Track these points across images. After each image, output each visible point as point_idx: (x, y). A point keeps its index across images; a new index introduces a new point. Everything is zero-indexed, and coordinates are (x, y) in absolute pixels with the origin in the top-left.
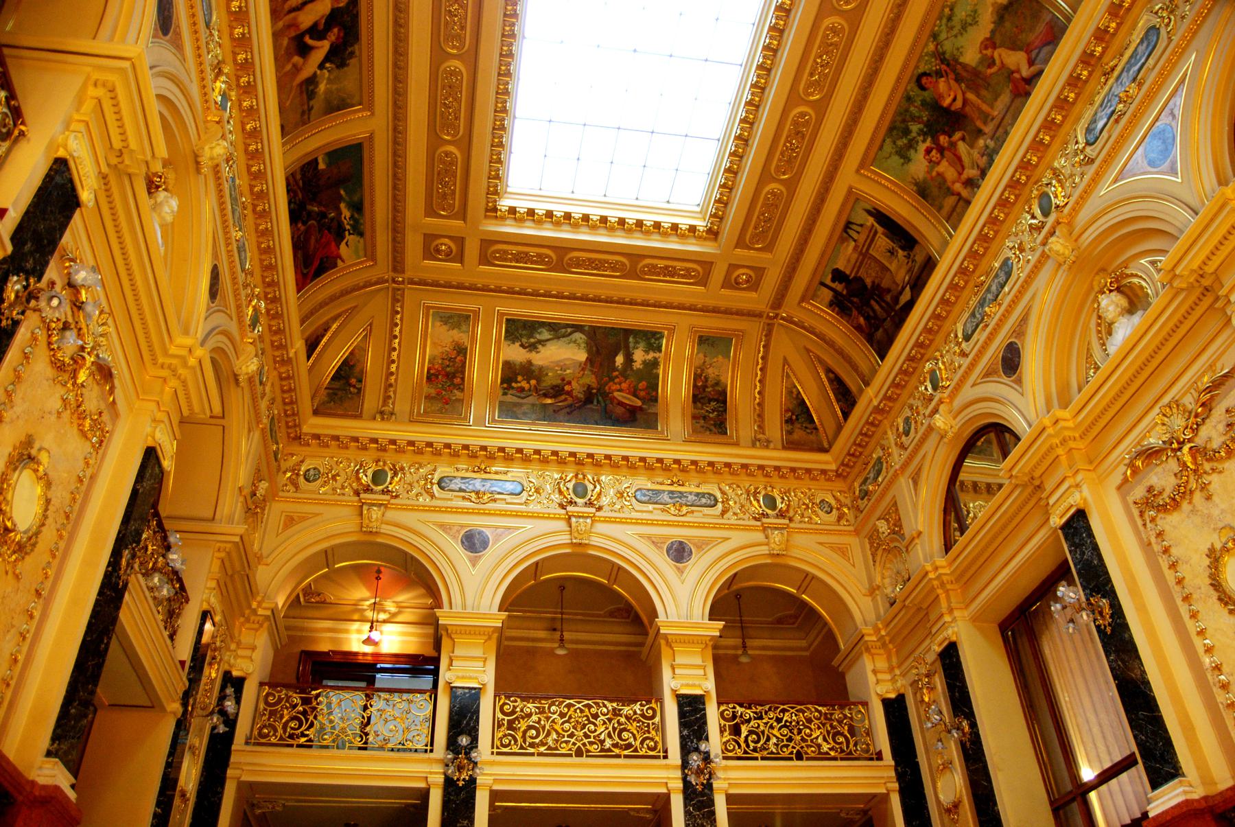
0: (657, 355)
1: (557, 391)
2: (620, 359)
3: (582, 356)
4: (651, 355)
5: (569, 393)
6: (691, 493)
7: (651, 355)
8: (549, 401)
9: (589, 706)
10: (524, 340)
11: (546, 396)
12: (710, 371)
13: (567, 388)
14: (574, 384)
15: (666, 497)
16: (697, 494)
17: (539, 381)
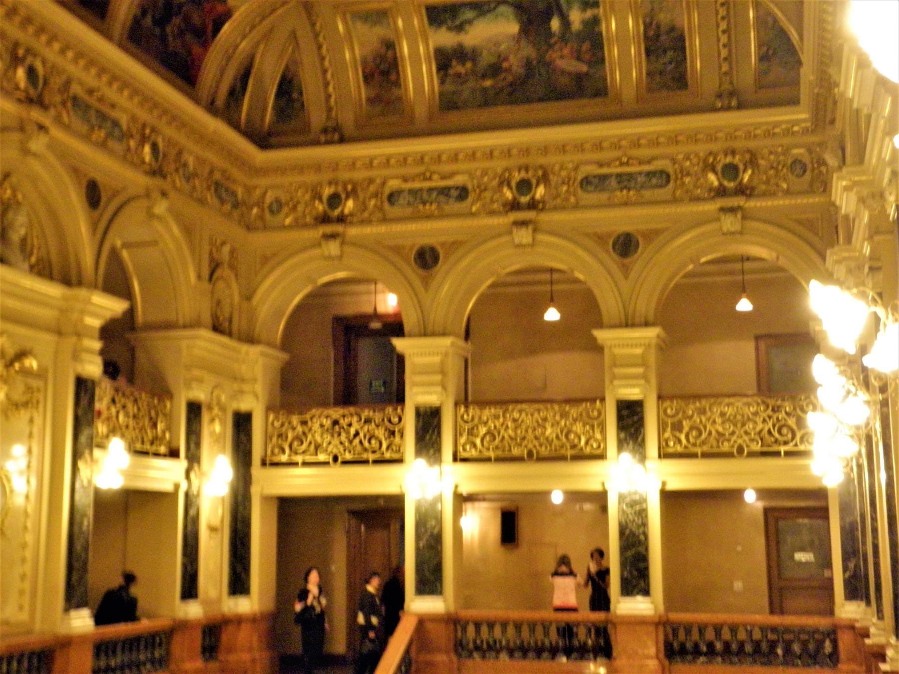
0: (595, 11)
1: (495, 70)
2: (555, 24)
3: (514, 28)
4: (589, 14)
5: (508, 70)
6: (640, 173)
7: (589, 14)
8: (488, 83)
9: (539, 411)
10: (449, 23)
11: (484, 77)
12: (662, 16)
13: (505, 65)
14: (512, 58)
15: (613, 182)
16: (649, 174)
17: (474, 60)
